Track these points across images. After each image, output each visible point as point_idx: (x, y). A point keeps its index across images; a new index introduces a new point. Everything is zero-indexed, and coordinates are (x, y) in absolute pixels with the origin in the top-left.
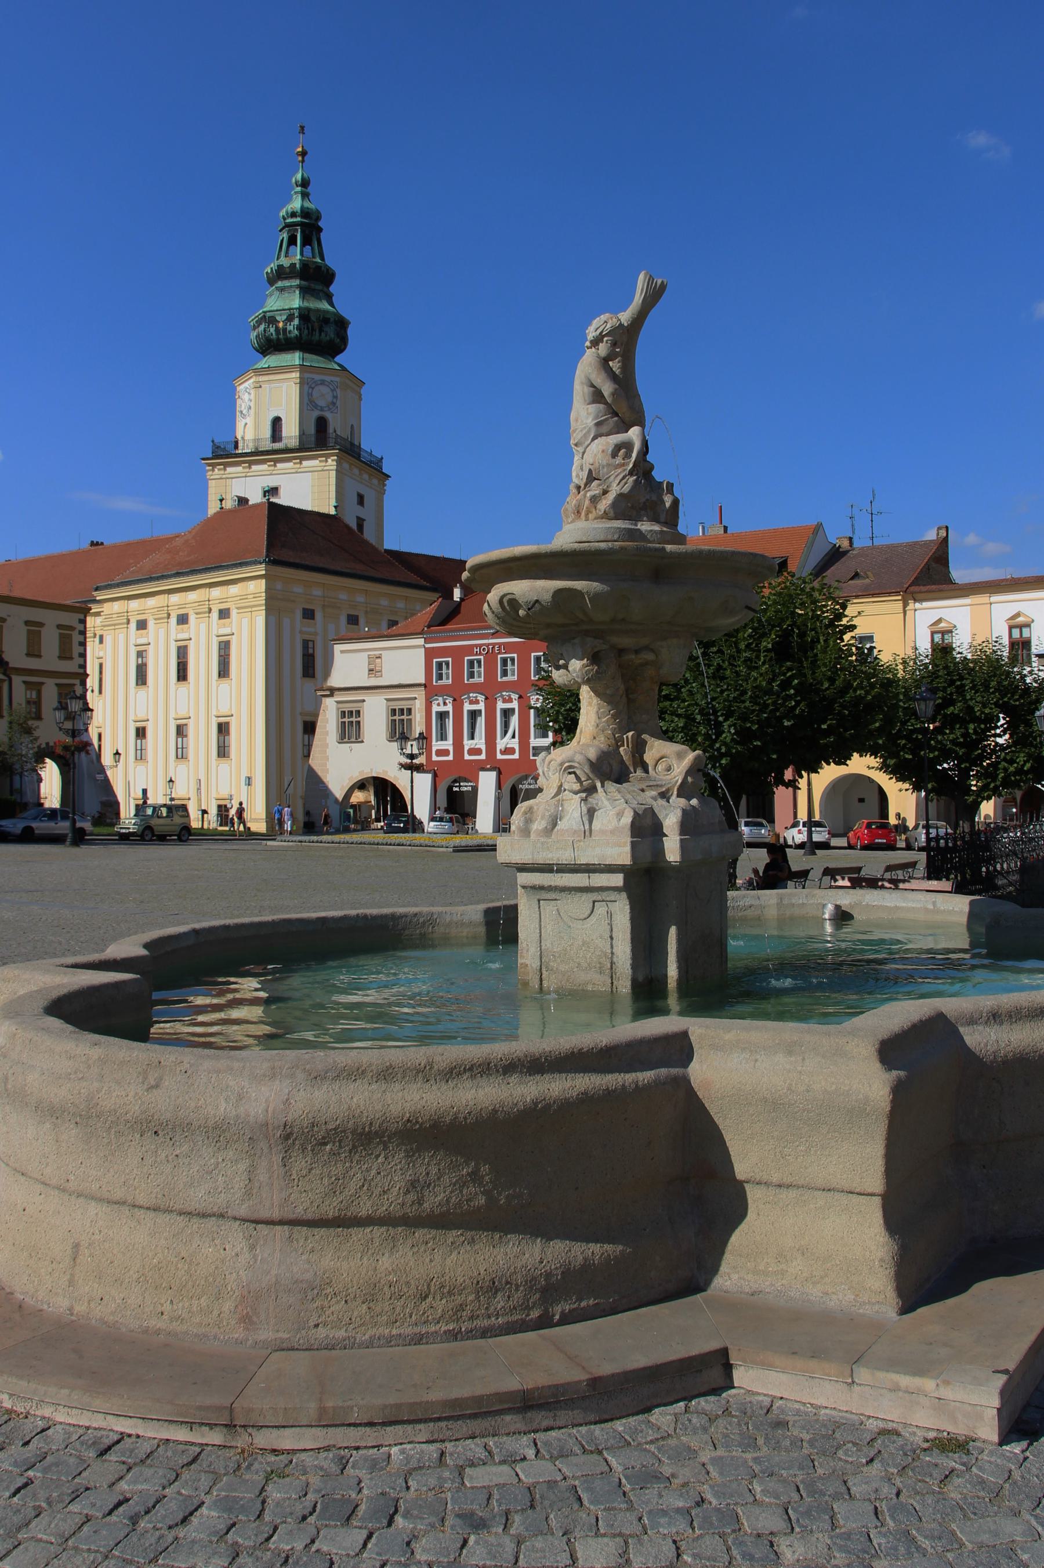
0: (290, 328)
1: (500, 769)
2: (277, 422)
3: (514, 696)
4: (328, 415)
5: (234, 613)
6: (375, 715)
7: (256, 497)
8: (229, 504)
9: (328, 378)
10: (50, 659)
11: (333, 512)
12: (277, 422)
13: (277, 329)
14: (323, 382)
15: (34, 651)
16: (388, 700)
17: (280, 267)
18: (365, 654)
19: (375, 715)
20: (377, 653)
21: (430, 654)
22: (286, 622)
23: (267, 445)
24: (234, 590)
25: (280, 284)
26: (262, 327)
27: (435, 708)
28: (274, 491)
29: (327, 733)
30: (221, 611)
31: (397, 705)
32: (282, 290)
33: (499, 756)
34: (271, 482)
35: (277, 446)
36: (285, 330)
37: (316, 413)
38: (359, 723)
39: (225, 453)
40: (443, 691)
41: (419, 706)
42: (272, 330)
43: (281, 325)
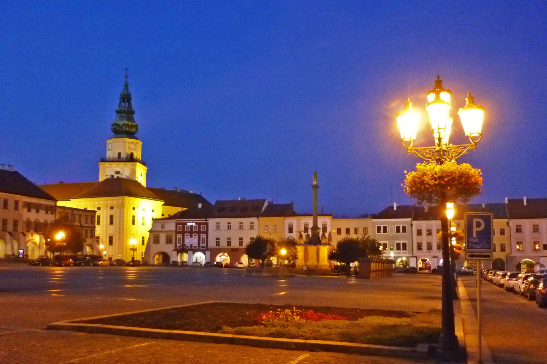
4: (133, 152)
6: (163, 238)
7: (116, 176)
8: (109, 177)
10: (89, 225)
14: (132, 143)
15: (86, 223)
17: (121, 110)
19: (163, 238)
21: (177, 224)
23: (117, 160)
26: (115, 126)
27: (178, 237)
28: (118, 173)
34: (118, 169)
35: (120, 160)
39: (104, 160)
41: (174, 236)
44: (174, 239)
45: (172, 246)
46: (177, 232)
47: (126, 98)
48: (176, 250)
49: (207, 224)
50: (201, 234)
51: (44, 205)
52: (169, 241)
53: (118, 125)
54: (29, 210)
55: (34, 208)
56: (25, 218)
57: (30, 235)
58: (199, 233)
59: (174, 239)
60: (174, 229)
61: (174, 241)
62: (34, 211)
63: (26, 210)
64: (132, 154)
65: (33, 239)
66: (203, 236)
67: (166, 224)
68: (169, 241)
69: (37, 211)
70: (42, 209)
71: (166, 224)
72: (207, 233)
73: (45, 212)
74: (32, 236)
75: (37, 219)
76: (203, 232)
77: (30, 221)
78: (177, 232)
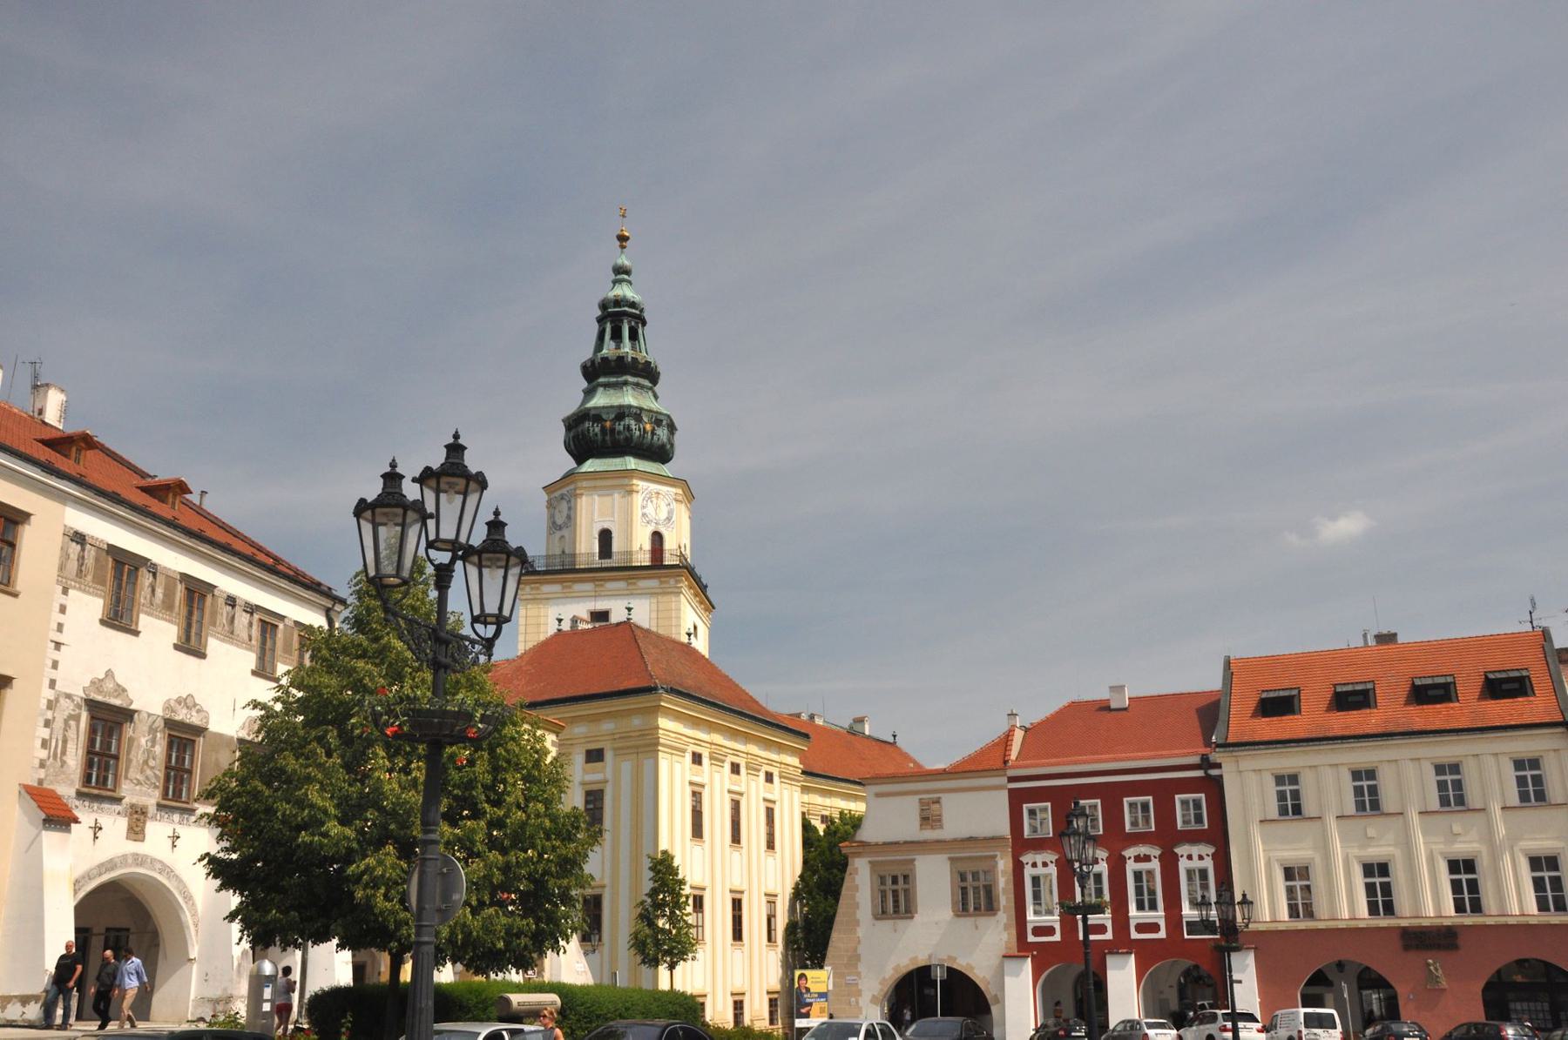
0: (620, 427)
1: (1147, 955)
2: (605, 537)
3: (1155, 852)
4: (662, 530)
5: (608, 755)
6: (933, 880)
8: (566, 626)
9: (664, 489)
11: (685, 639)
12: (605, 537)
13: (603, 429)
16: (951, 859)
17: (605, 359)
18: (917, 798)
20: (936, 795)
21: (1017, 799)
22: (677, 767)
23: (597, 562)
24: (608, 726)
25: (601, 380)
29: (857, 906)
30: (589, 753)
31: (968, 868)
32: (606, 386)
33: (1134, 935)
34: (601, 605)
35: (606, 563)
36: (613, 430)
37: (651, 528)
38: (906, 891)
40: (1038, 845)
41: (1004, 864)
42: (597, 430)
43: (608, 424)
44: (1003, 882)
45: (995, 933)
46: (1020, 845)
47: (619, 318)
48: (1023, 947)
49: (1214, 788)
50: (1182, 850)
51: (252, 609)
52: (973, 898)
53: (596, 416)
54: (119, 618)
55: (168, 605)
56: (76, 677)
57: (115, 824)
58: (1168, 838)
59: (1003, 882)
60: (1004, 828)
61: (1005, 899)
62: (158, 631)
63: (88, 606)
64: (657, 537)
65: (139, 859)
66: (1194, 858)
67: (945, 798)
68: (973, 898)
69: (190, 645)
70: (230, 635)
71: (945, 798)
72: (1218, 836)
73: (250, 659)
74: (136, 832)
75: (187, 702)
76: (1193, 837)
77: (127, 715)
78: (1020, 845)
